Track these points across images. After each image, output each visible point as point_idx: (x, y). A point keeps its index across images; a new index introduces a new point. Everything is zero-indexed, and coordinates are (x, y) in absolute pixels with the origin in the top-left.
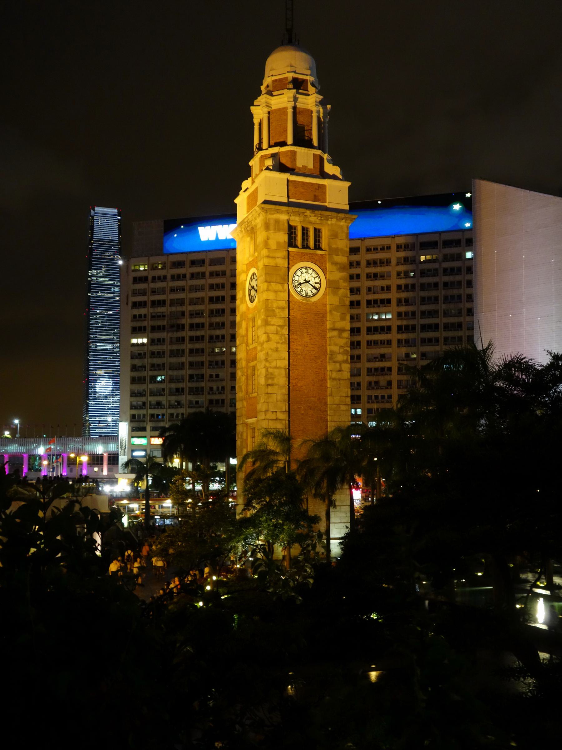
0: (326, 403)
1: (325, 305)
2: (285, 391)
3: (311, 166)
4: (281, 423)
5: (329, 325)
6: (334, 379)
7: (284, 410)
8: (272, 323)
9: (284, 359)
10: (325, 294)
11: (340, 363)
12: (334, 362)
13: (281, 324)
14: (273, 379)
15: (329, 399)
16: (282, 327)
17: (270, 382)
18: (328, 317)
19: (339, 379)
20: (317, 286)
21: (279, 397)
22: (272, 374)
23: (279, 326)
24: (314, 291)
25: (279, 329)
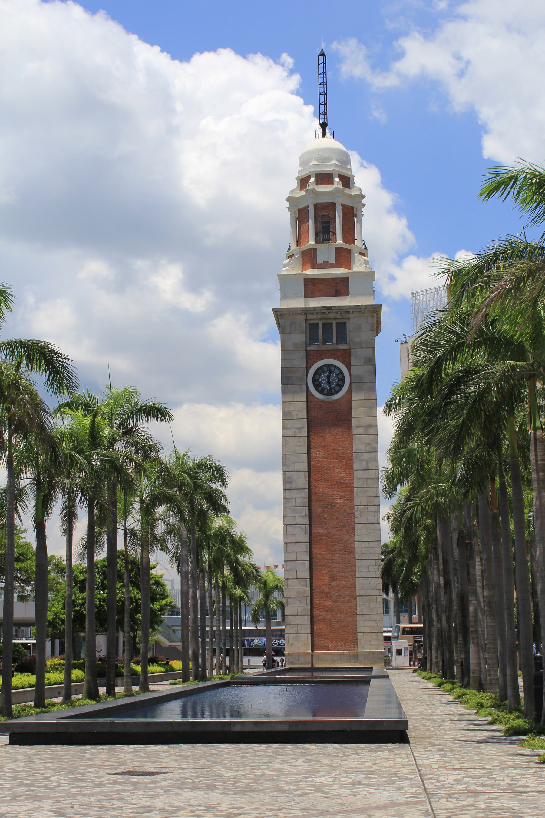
0: (352, 506)
1: (350, 401)
2: (305, 494)
3: (333, 260)
4: (300, 527)
5: (355, 422)
6: (359, 479)
7: (303, 514)
8: (289, 426)
9: (303, 462)
10: (350, 391)
11: (367, 461)
12: (359, 460)
13: (299, 426)
14: (291, 483)
16: (300, 429)
17: (288, 486)
18: (354, 414)
20: (340, 383)
21: (298, 501)
22: (290, 478)
23: (296, 428)
25: (297, 431)
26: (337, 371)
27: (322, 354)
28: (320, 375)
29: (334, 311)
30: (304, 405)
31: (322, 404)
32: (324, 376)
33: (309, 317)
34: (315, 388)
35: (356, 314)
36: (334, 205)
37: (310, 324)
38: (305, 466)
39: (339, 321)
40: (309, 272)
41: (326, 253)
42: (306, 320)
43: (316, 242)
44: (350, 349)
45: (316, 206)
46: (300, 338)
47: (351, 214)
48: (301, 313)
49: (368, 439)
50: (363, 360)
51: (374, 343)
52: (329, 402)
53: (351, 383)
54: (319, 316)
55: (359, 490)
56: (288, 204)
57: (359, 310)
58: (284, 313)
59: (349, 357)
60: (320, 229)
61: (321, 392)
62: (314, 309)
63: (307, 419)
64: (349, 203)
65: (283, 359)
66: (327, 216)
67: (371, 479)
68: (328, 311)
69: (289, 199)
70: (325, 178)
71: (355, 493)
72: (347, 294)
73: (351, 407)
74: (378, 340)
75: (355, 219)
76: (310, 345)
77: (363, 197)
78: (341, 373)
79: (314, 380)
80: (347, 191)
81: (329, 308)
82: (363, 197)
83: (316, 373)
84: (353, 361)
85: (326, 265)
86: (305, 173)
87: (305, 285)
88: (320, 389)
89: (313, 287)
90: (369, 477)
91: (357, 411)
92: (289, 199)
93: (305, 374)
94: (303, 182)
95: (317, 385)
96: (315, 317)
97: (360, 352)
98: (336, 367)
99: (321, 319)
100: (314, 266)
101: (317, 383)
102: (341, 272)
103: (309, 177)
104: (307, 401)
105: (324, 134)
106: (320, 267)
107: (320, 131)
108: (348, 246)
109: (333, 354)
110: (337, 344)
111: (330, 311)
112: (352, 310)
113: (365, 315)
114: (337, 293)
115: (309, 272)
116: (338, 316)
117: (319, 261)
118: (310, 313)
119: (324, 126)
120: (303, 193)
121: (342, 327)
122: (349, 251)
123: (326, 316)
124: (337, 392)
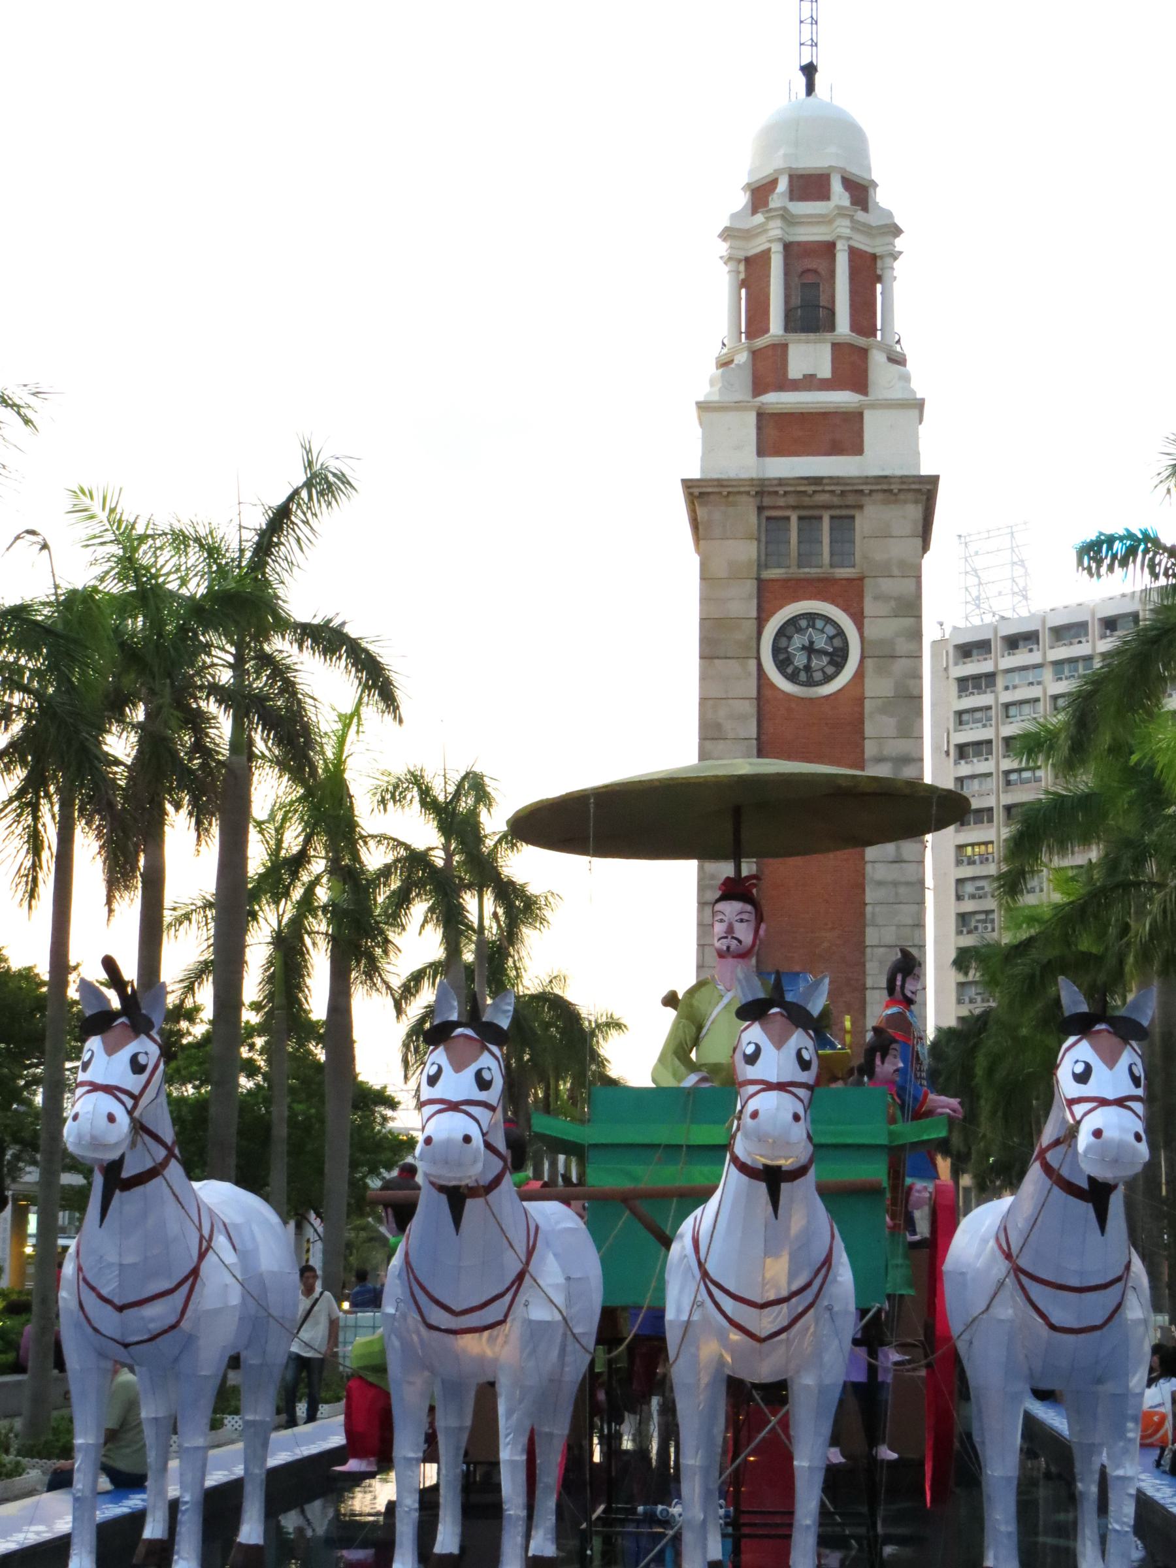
0: (861, 947)
1: (860, 700)
3: (825, 372)
6: (880, 883)
10: (860, 674)
15: (869, 931)
18: (869, 729)
19: (895, 884)
24: (830, 670)
26: (831, 631)
27: (796, 588)
28: (790, 638)
29: (827, 488)
30: (750, 708)
31: (793, 705)
32: (798, 641)
33: (767, 501)
34: (778, 668)
35: (879, 497)
36: (829, 249)
37: (768, 519)
39: (837, 512)
41: (810, 357)
42: (760, 509)
43: (787, 329)
44: (861, 579)
45: (788, 247)
46: (746, 551)
47: (869, 271)
48: (748, 493)
50: (893, 603)
51: (919, 568)
52: (811, 700)
53: (863, 658)
54: (792, 500)
55: (878, 909)
56: (723, 248)
57: (885, 487)
58: (709, 490)
59: (861, 596)
60: (796, 301)
61: (792, 678)
62: (781, 482)
63: (758, 739)
64: (864, 244)
65: (705, 600)
66: (815, 271)
67: (908, 884)
68: (813, 488)
69: (728, 234)
70: (810, 185)
71: (868, 916)
72: (857, 449)
73: (862, 714)
74: (929, 563)
75: (879, 287)
76: (767, 567)
77: (897, 231)
78: (841, 633)
79: (776, 650)
80: (861, 216)
81: (817, 480)
82: (897, 231)
83: (781, 633)
84: (870, 607)
85: (810, 382)
86: (766, 171)
87: (759, 428)
88: (790, 670)
90: (903, 880)
92: (728, 234)
93: (755, 634)
94: (760, 194)
95: (783, 662)
96: (781, 502)
97: (887, 585)
98: (828, 620)
99: (794, 508)
100: (785, 384)
101: (782, 657)
103: (772, 184)
104: (759, 697)
105: (810, 89)
106: (795, 386)
107: (802, 80)
108: (861, 341)
109: (823, 588)
110: (832, 566)
111: (819, 488)
112: (869, 487)
113: (902, 497)
114: (836, 449)
116: (836, 500)
117: (795, 371)
118: (770, 493)
119: (809, 71)
120: (759, 218)
121: (844, 523)
122: (864, 352)
123: (807, 501)
124: (828, 679)
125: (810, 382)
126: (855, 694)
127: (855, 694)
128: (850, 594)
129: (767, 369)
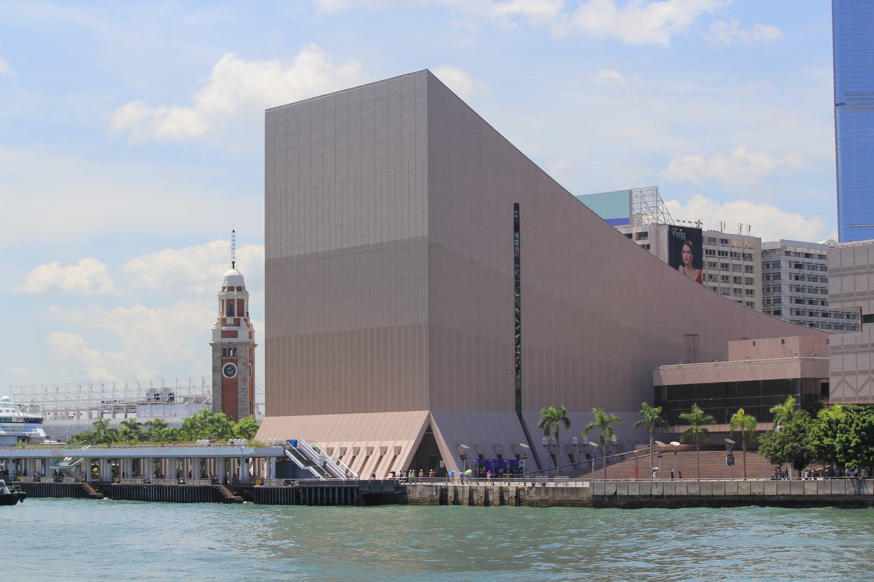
27: (228, 361)
36: (233, 300)
38: (220, 403)
40: (224, 328)
41: (230, 320)
46: (220, 354)
49: (243, 393)
70: (231, 289)
85: (230, 325)
89: (225, 334)
91: (240, 383)
94: (224, 288)
95: (226, 373)
100: (226, 325)
102: (234, 328)
109: (232, 361)
114: (234, 337)
115: (224, 328)
119: (233, 263)
125: (230, 325)
126: (237, 378)
127: (237, 378)
128: (236, 362)
129: (223, 322)
